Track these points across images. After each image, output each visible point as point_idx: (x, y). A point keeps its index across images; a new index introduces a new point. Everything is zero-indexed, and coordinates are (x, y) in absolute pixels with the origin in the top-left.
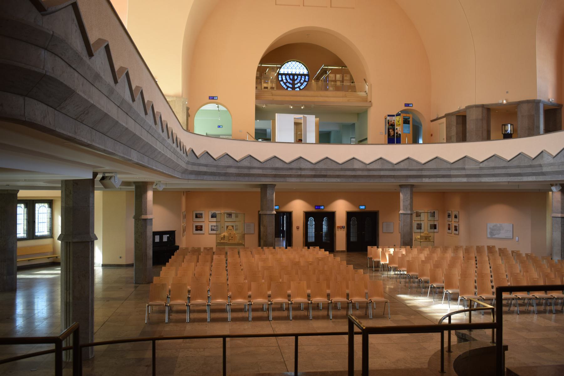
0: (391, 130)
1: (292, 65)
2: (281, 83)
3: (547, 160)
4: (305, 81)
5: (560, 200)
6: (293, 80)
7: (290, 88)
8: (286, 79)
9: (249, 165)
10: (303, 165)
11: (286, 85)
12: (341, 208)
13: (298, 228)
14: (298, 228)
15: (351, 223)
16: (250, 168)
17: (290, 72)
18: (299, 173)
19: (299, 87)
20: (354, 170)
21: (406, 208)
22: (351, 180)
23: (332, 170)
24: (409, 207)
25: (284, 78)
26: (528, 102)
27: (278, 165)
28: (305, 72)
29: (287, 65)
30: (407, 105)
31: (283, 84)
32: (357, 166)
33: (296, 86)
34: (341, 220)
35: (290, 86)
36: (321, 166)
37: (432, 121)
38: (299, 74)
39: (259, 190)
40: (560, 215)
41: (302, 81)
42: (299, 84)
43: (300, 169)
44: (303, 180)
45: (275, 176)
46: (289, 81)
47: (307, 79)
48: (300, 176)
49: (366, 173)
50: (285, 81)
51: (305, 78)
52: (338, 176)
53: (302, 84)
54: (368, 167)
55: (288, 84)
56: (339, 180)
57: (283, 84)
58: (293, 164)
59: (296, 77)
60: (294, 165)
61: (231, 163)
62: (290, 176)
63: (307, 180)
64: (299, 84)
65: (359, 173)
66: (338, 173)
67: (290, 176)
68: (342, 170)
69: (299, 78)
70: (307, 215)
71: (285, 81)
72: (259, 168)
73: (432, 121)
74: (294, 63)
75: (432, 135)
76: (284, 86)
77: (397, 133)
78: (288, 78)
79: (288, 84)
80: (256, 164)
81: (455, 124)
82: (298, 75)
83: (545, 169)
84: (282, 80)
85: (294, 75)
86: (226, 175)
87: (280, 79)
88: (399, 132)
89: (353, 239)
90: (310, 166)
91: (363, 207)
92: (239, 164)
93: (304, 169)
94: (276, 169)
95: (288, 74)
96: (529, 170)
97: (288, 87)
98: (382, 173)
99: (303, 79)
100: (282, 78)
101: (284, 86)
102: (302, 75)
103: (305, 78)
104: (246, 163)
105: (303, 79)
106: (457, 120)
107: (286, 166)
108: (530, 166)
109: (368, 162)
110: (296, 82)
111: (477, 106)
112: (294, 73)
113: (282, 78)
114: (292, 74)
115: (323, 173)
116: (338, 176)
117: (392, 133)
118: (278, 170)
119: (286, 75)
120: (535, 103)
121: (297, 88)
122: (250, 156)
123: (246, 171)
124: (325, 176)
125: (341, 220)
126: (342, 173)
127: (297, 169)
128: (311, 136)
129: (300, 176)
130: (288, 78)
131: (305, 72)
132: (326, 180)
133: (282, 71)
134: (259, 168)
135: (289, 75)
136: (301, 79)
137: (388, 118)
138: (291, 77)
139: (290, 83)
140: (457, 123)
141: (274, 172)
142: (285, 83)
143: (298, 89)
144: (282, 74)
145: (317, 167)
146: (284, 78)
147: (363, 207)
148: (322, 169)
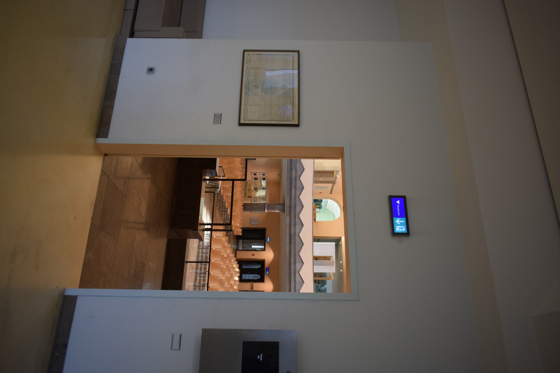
9: (298, 187)
10: (298, 227)
16: (295, 187)
20: (295, 263)
22: (288, 262)
23: (295, 247)
32: (298, 265)
36: (298, 240)
39: (281, 203)
43: (295, 224)
44: (288, 228)
45: (290, 207)
48: (290, 225)
49: (292, 271)
52: (290, 252)
54: (297, 274)
56: (288, 253)
58: (299, 219)
60: (297, 220)
61: (299, 173)
62: (290, 218)
63: (288, 231)
67: (290, 218)
68: (295, 254)
72: (295, 194)
80: (298, 193)
86: (291, 168)
90: (297, 232)
92: (298, 179)
93: (295, 227)
94: (295, 207)
98: (293, 283)
104: (298, 185)
107: (297, 214)
115: (293, 241)
116: (290, 252)
118: (295, 243)
123: (293, 185)
124: (290, 243)
127: (295, 222)
128: (319, 269)
129: (290, 225)
132: (288, 244)
134: (295, 194)
141: (293, 205)
145: (297, 237)
148: (295, 239)
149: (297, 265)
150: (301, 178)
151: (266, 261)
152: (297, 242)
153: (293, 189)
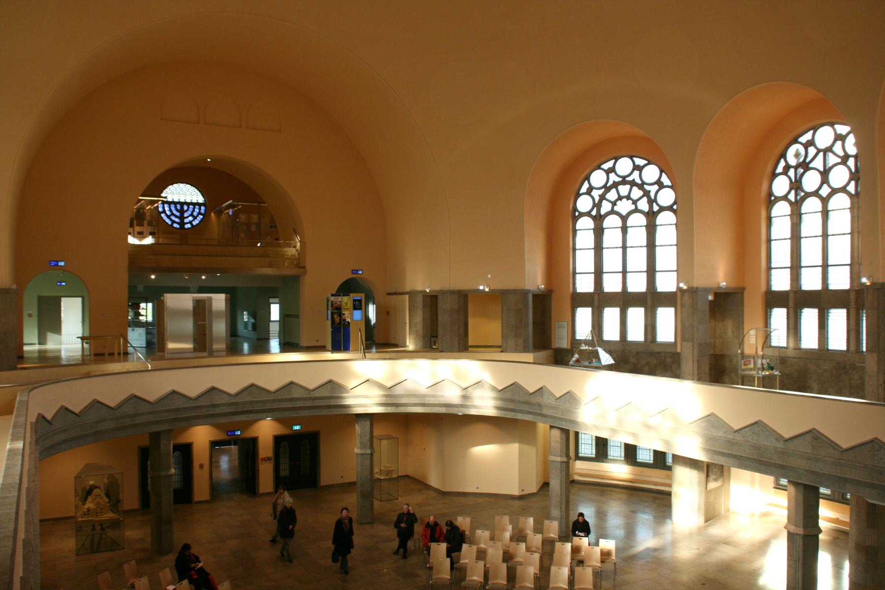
0: (335, 316)
2: (163, 215)
3: (546, 400)
4: (199, 213)
5: (559, 439)
6: (182, 212)
8: (170, 210)
10: (218, 400)
11: (171, 220)
12: (266, 430)
13: (201, 466)
14: (201, 466)
15: (281, 450)
17: (176, 200)
18: (212, 412)
19: (190, 222)
20: (292, 400)
21: (363, 446)
24: (369, 443)
25: (167, 208)
26: (515, 292)
27: (179, 403)
28: (201, 199)
30: (355, 272)
31: (165, 218)
33: (186, 221)
34: (266, 448)
35: (177, 220)
37: (389, 294)
38: (192, 203)
40: (559, 459)
41: (195, 214)
42: (191, 218)
43: (214, 406)
45: (174, 420)
47: (203, 211)
49: (309, 404)
50: (168, 213)
51: (200, 209)
53: (195, 218)
54: (313, 395)
55: (173, 218)
57: (165, 218)
59: (185, 208)
60: (202, 402)
65: (300, 404)
66: (269, 406)
70: (214, 444)
71: (168, 213)
72: (148, 413)
73: (389, 294)
74: (182, 185)
75: (388, 313)
76: (168, 221)
77: (345, 320)
78: (173, 208)
79: (173, 218)
81: (421, 306)
82: (188, 204)
83: (545, 412)
84: (164, 212)
85: (182, 204)
87: (161, 209)
88: (348, 320)
89: (285, 471)
91: (297, 428)
93: (219, 405)
96: (525, 408)
97: (174, 222)
99: (197, 210)
100: (164, 208)
101: (168, 221)
102: (194, 204)
103: (200, 209)
105: (197, 210)
106: (424, 300)
108: (527, 403)
109: (311, 386)
110: (186, 215)
111: (452, 292)
112: (182, 200)
113: (164, 208)
114: (179, 203)
117: (337, 319)
120: (524, 293)
122: (135, 396)
125: (266, 448)
126: (275, 406)
127: (208, 406)
130: (173, 208)
131: (201, 199)
135: (175, 203)
136: (194, 211)
137: (332, 299)
138: (179, 207)
139: (176, 216)
140: (424, 306)
142: (168, 217)
145: (238, 400)
146: (167, 208)
147: (297, 428)
149: (295, 394)
150: (112, 404)
151: (213, 439)
152: (248, 399)
153: (138, 420)
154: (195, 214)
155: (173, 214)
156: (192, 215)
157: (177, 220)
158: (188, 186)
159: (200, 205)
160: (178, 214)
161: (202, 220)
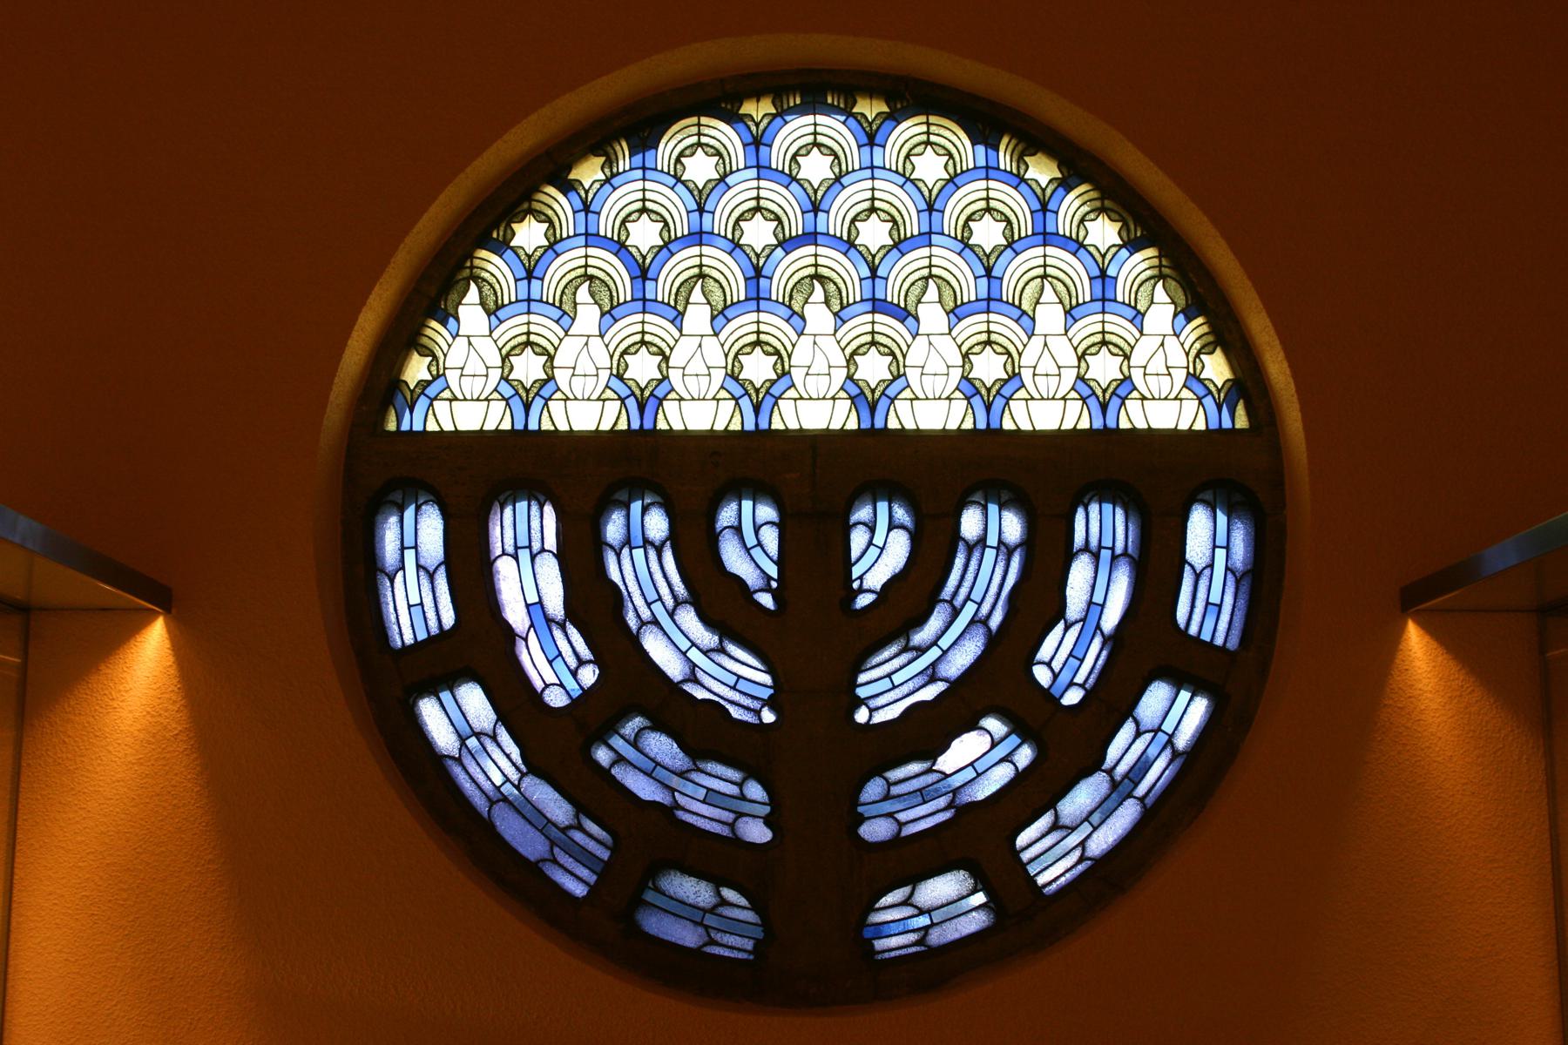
1: (754, 212)
4: (1151, 645)
6: (817, 630)
7: (716, 857)
8: (594, 604)
19: (978, 837)
25: (528, 583)
28: (1168, 378)
29: (631, 197)
33: (897, 806)
35: (716, 797)
38: (988, 461)
41: (1065, 661)
42: (980, 758)
46: (676, 645)
47: (1208, 606)
50: (557, 668)
51: (1157, 567)
53: (1065, 744)
55: (645, 760)
59: (880, 551)
64: (980, 758)
69: (984, 583)
71: (557, 668)
74: (812, 140)
78: (643, 571)
82: (937, 475)
84: (478, 644)
85: (815, 479)
87: (416, 605)
95: (641, 463)
99: (1098, 591)
100: (469, 568)
102: (1048, 476)
103: (1157, 567)
105: (1098, 591)
110: (889, 688)
113: (469, 568)
119: (584, 477)
121: (915, 858)
130: (643, 571)
131: (1168, 378)
133: (465, 379)
135: (685, 474)
136: (1036, 603)
138: (751, 541)
143: (950, 900)
144: (477, 477)
146: (528, 583)
154: (1065, 661)
155: (630, 685)
156: (998, 682)
157: (716, 797)
158: (930, 150)
159: (1147, 475)
160: (737, 679)
161: (1201, 765)
